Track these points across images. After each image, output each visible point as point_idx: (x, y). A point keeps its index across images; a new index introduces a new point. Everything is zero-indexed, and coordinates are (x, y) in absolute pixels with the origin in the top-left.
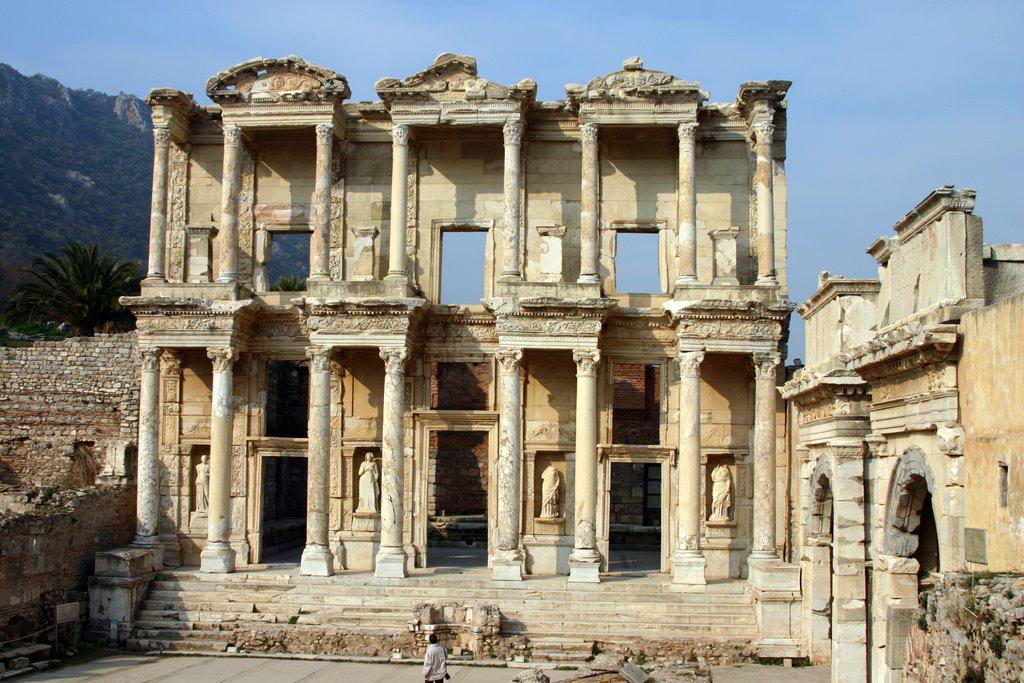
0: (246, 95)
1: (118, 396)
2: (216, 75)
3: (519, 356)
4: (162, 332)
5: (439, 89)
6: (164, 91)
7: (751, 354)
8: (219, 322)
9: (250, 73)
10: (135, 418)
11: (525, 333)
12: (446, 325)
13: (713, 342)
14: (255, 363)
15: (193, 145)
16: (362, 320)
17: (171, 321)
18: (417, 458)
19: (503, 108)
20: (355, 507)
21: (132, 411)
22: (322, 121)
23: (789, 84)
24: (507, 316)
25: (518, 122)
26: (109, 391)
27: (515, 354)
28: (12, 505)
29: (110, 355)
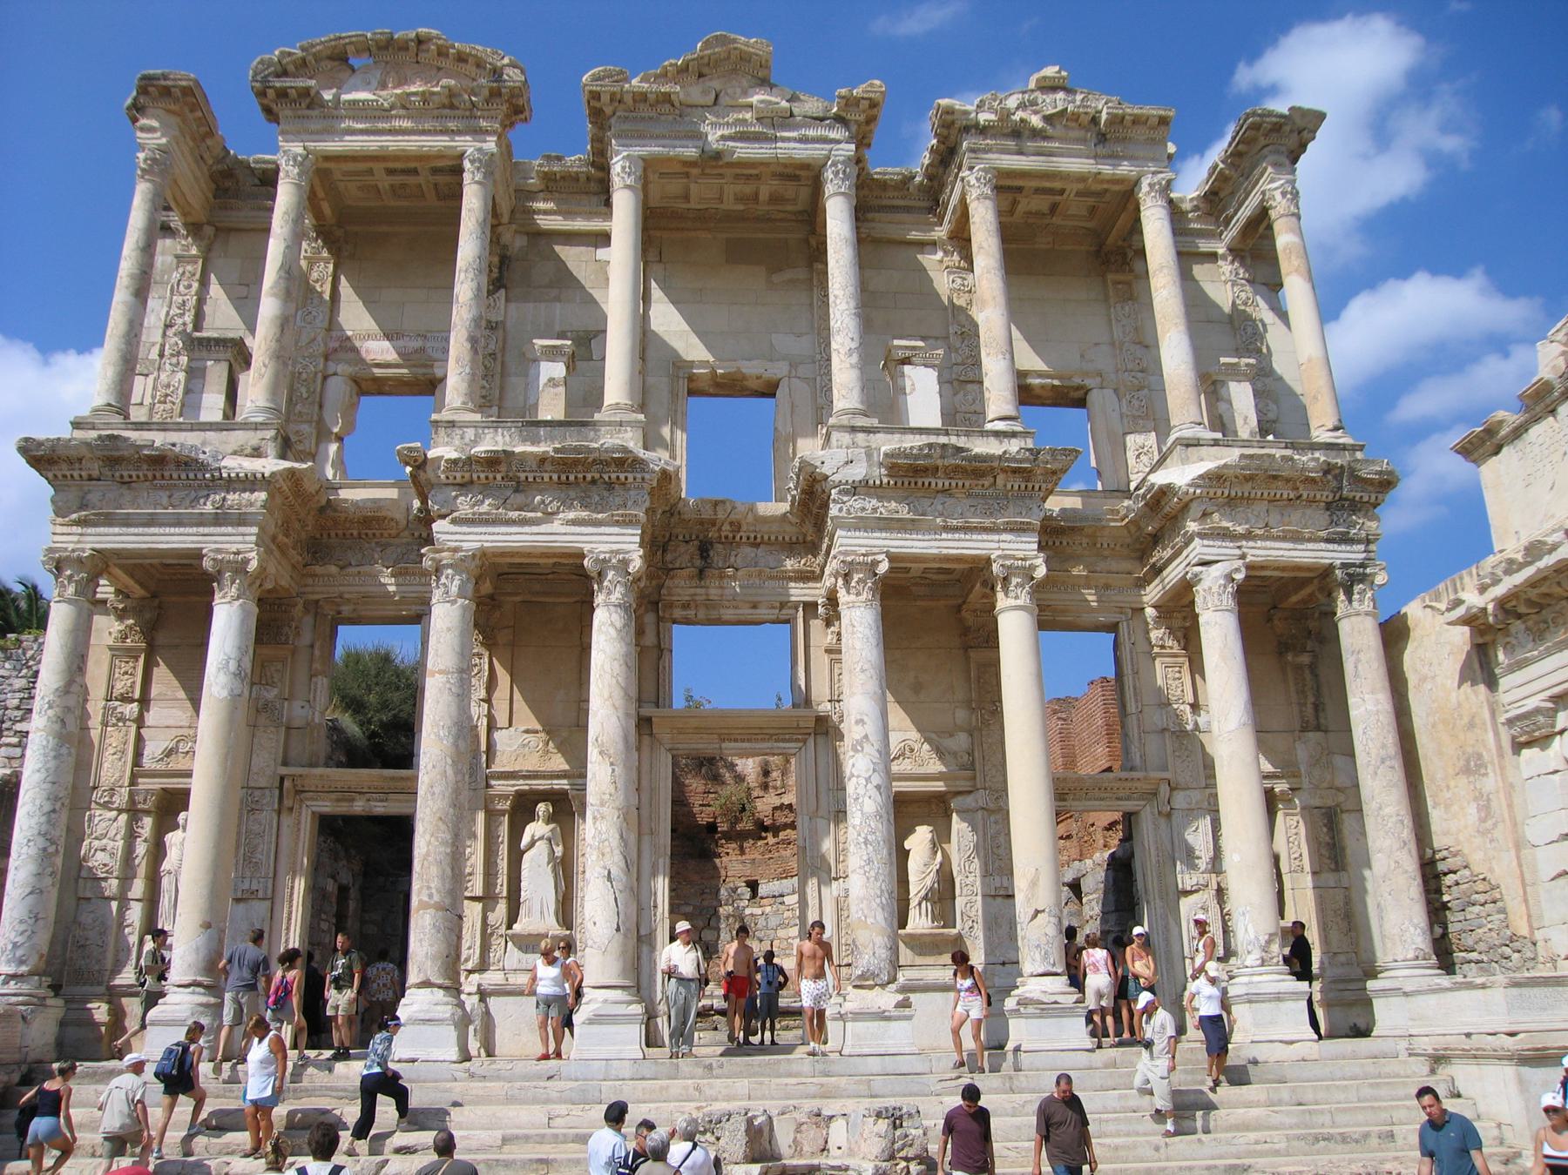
0: (328, 95)
3: (883, 567)
5: (702, 101)
6: (165, 77)
7: (1330, 569)
9: (339, 60)
12: (704, 549)
13: (1259, 543)
14: (308, 620)
15: (217, 229)
18: (645, 812)
20: (512, 918)
23: (1320, 117)
24: (855, 489)
25: (849, 158)
27: (875, 563)
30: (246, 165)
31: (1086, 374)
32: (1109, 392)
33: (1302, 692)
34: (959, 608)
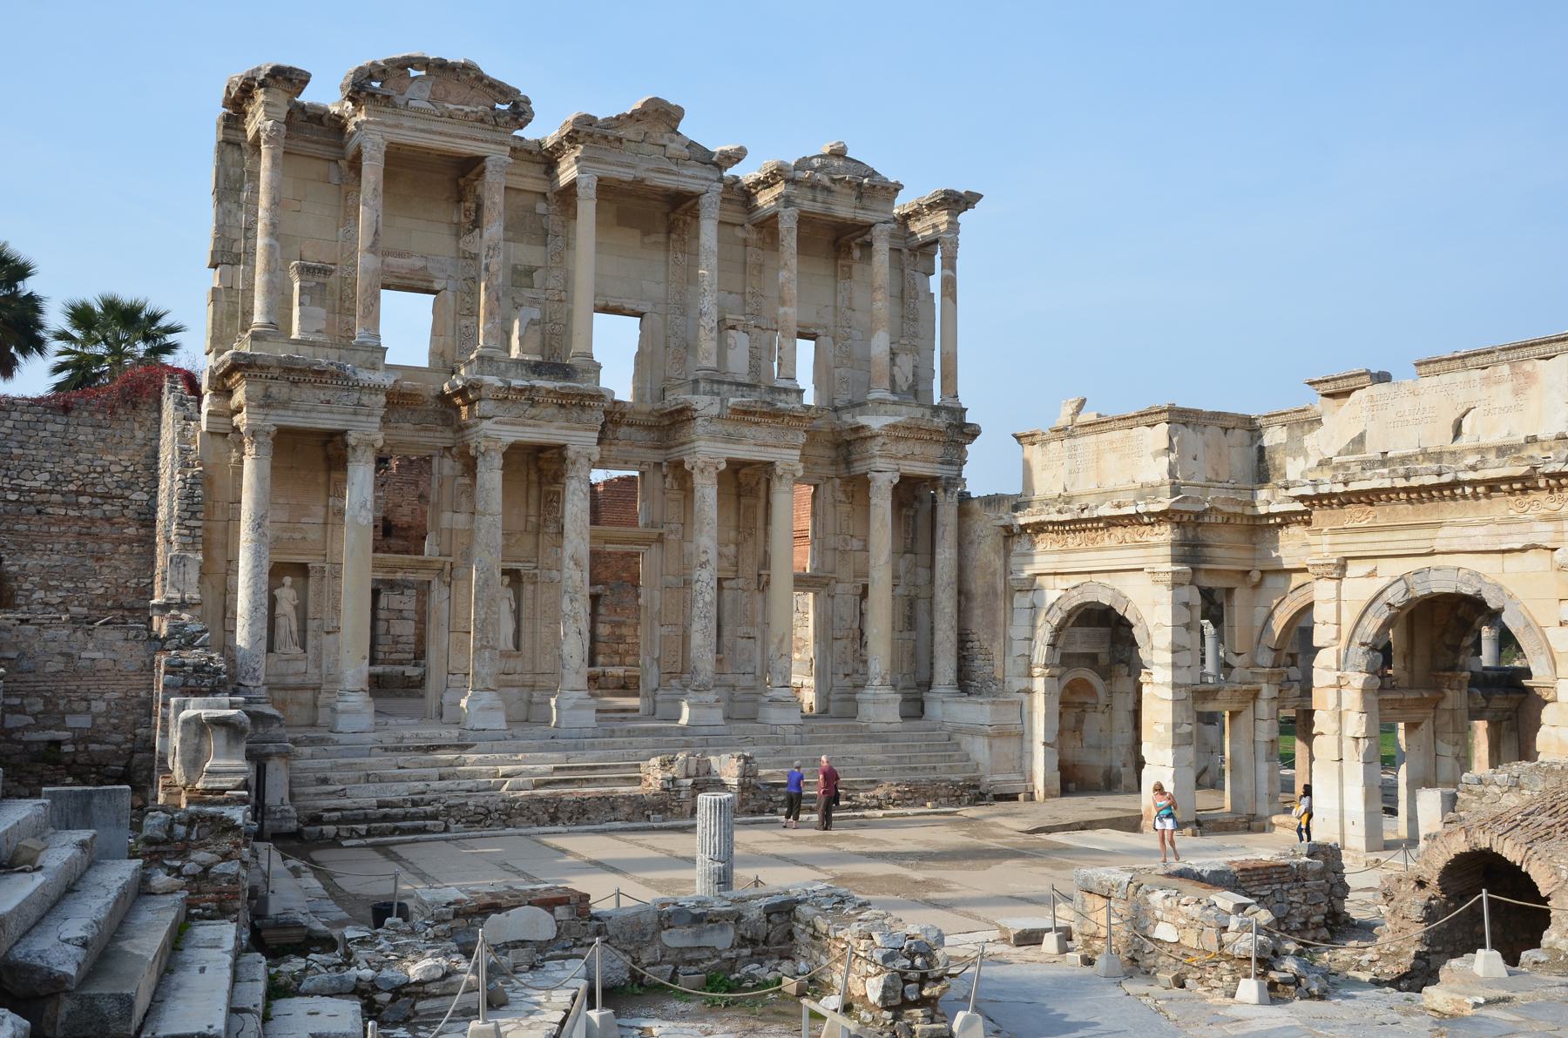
0: (400, 101)
1: (45, 492)
2: (365, 61)
3: (723, 466)
4: (285, 405)
6: (291, 70)
8: (365, 399)
10: (199, 523)
11: (729, 438)
16: (551, 410)
17: (296, 391)
19: (705, 174)
21: (194, 513)
22: (496, 156)
24: (711, 420)
26: (28, 484)
28: (120, 644)
29: (31, 432)
30: (302, 108)
31: (818, 326)
32: (829, 339)
33: (906, 531)
34: (736, 472)
